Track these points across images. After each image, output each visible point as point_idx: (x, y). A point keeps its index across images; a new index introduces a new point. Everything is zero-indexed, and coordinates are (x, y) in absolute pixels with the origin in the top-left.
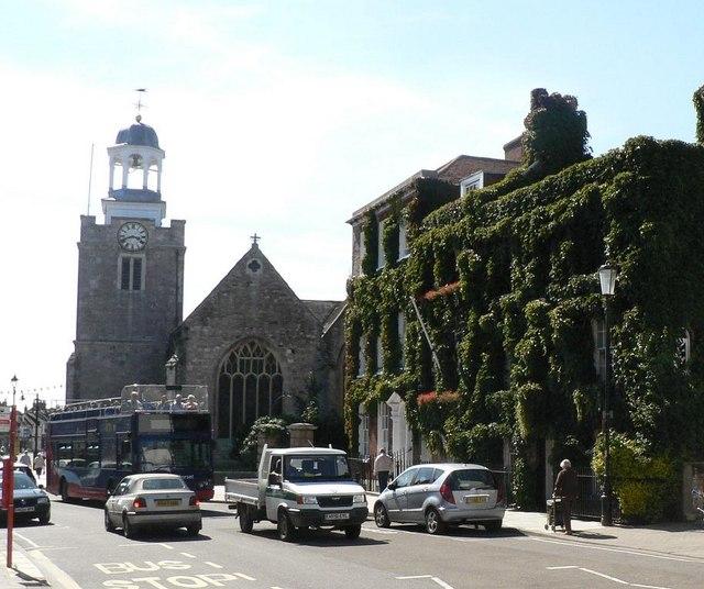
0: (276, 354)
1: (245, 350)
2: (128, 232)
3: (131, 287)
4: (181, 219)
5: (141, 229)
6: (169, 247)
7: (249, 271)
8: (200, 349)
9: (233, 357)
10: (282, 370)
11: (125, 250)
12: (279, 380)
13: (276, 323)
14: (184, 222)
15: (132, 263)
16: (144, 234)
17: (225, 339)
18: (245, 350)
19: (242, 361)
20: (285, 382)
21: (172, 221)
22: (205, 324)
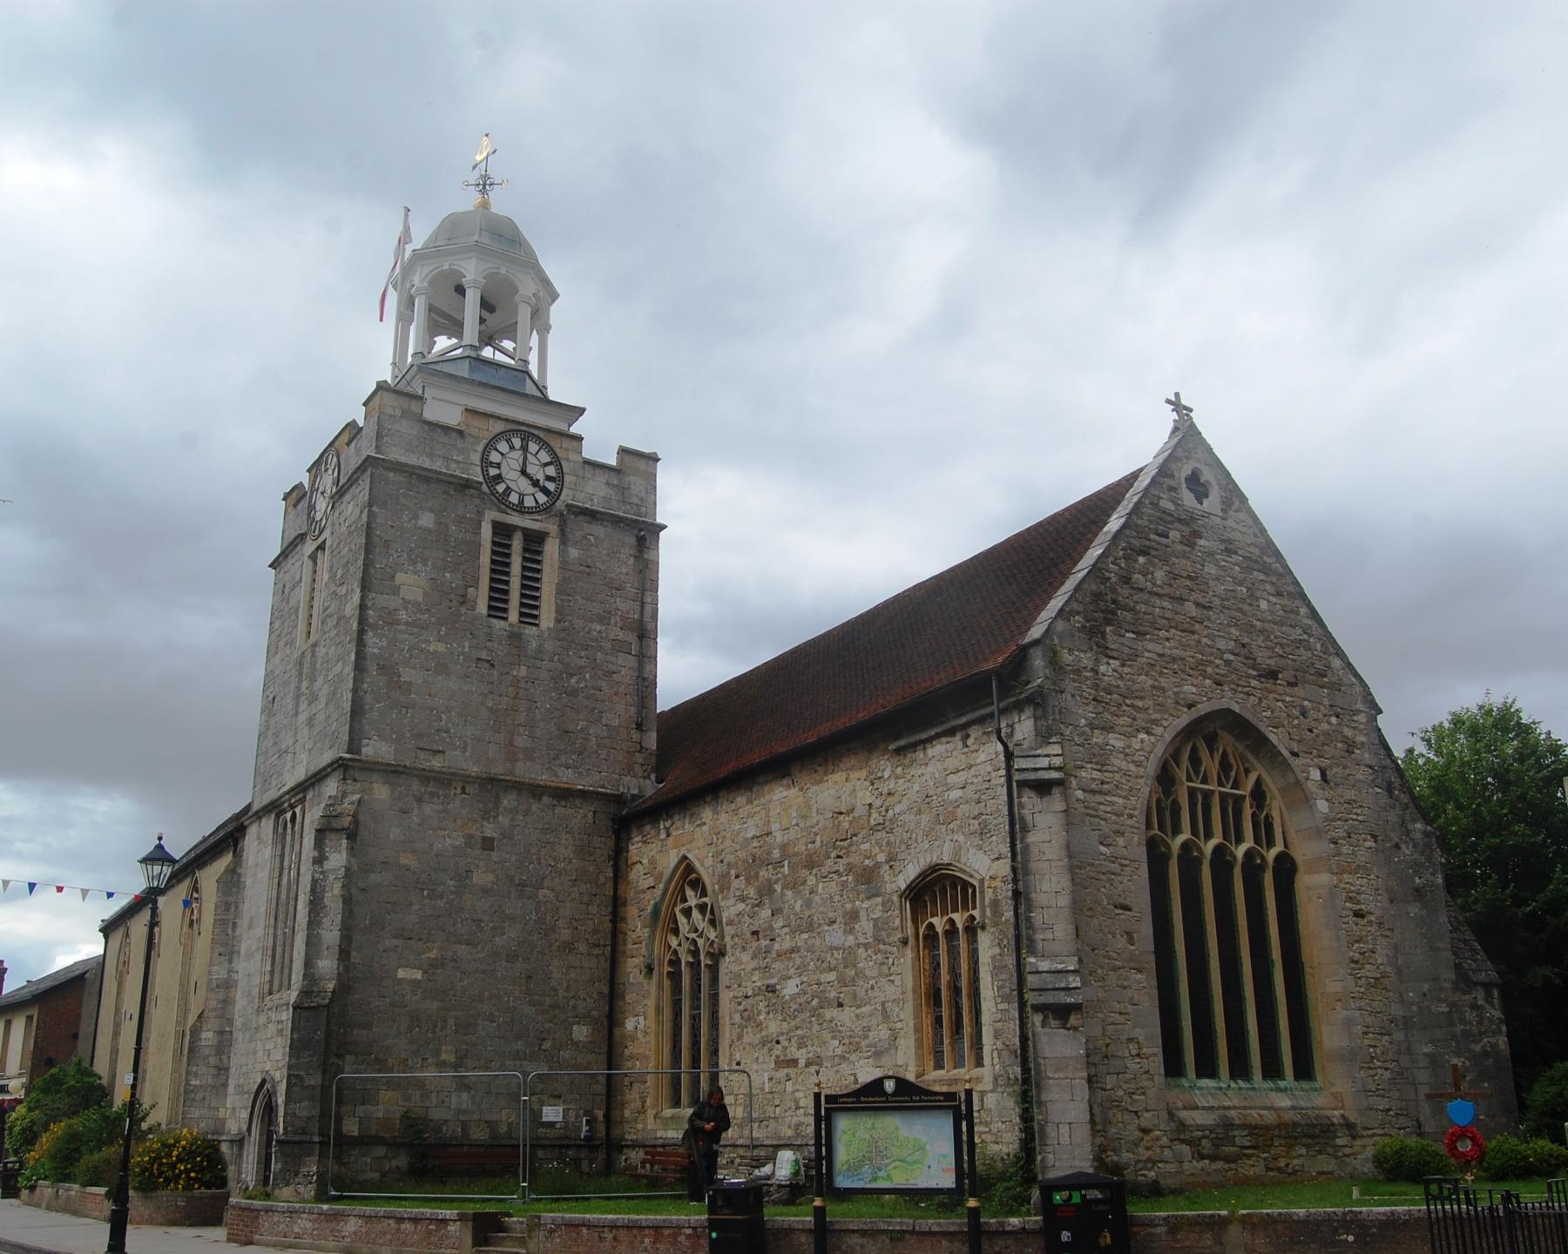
0: (1272, 785)
1: (1195, 761)
2: (509, 462)
3: (513, 616)
4: (646, 450)
5: (544, 457)
7: (1188, 498)
8: (1097, 738)
9: (1165, 778)
10: (1292, 835)
11: (502, 501)
12: (1286, 868)
13: (1272, 675)
14: (654, 459)
15: (517, 544)
16: (551, 471)
17: (1160, 706)
18: (1195, 761)
19: (1192, 792)
21: (624, 452)
22: (1105, 652)
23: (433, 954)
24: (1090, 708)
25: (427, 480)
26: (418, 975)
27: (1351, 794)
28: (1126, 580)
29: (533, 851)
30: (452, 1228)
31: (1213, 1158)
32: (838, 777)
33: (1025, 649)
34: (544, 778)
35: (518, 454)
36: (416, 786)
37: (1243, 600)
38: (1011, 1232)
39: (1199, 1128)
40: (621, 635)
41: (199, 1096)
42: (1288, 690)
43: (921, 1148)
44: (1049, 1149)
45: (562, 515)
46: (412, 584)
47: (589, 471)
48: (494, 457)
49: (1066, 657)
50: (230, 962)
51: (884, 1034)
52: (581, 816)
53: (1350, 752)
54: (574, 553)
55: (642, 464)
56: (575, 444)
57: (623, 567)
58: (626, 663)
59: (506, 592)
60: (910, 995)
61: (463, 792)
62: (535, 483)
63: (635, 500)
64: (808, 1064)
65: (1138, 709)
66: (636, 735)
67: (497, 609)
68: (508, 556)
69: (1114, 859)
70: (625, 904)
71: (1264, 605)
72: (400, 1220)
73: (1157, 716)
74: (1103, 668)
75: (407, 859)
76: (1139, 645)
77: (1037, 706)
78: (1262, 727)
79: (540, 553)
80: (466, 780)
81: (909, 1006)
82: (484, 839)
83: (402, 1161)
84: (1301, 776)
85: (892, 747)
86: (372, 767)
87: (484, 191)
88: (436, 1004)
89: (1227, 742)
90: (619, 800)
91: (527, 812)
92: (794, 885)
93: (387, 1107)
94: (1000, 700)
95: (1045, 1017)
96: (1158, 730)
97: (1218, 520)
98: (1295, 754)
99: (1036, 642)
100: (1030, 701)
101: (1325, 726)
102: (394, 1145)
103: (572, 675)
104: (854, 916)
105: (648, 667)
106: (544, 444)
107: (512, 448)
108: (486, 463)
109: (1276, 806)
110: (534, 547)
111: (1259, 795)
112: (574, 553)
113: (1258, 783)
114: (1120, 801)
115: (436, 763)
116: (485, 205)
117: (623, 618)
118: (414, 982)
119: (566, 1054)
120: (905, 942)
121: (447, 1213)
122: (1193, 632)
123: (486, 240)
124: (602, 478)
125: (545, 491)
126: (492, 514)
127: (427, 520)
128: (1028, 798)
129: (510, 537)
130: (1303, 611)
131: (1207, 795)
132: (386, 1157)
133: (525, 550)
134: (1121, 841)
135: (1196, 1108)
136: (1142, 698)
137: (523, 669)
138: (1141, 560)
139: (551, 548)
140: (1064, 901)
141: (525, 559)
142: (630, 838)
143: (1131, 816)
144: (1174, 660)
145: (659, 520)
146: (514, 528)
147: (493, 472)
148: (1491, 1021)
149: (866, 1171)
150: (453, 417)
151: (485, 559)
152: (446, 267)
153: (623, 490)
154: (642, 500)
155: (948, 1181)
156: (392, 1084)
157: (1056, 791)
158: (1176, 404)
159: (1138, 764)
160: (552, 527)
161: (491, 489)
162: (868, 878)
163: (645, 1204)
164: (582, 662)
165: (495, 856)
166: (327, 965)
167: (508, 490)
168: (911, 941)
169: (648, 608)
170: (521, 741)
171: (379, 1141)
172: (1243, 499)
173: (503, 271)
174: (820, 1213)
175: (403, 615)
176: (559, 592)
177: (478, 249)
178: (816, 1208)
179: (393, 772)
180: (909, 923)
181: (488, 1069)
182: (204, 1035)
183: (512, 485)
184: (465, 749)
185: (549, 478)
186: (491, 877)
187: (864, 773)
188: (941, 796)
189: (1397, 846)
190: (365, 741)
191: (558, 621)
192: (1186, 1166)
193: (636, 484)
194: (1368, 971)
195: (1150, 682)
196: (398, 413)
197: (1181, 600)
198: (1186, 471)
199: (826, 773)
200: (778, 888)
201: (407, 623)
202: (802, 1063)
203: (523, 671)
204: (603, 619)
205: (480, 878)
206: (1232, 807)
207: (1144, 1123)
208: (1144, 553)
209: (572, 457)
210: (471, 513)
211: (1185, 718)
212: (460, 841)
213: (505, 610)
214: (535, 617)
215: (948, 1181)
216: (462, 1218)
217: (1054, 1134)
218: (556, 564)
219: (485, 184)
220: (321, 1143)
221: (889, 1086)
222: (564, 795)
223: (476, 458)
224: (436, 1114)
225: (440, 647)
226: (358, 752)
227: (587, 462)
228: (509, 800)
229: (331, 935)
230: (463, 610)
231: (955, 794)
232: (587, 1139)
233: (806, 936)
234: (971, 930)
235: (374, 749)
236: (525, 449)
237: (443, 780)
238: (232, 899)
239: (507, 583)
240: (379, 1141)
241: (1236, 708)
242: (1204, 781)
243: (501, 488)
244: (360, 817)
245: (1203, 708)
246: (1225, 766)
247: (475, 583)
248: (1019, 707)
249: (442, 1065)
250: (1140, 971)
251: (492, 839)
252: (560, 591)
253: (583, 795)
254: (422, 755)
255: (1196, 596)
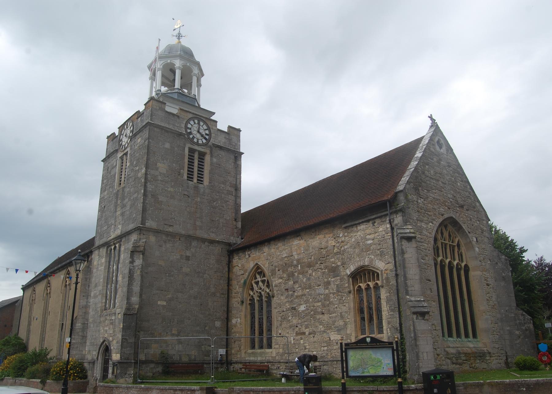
0: (462, 243)
1: (442, 234)
2: (194, 127)
3: (195, 180)
5: (205, 127)
6: (227, 149)
7: (437, 148)
9: (436, 240)
13: (462, 207)
14: (239, 130)
15: (196, 156)
16: (207, 132)
18: (442, 234)
20: (472, 274)
21: (230, 127)
23: (169, 296)
24: (417, 214)
25: (167, 132)
26: (165, 303)
27: (484, 246)
28: (423, 173)
29: (202, 261)
30: (197, 393)
31: (456, 364)
32: (321, 236)
33: (397, 193)
34: (206, 236)
35: (196, 125)
36: (164, 237)
37: (453, 182)
38: (412, 390)
39: (452, 354)
40: (230, 189)
41: (76, 346)
42: (467, 212)
43: (380, 361)
44: (420, 361)
45: (211, 147)
46: (162, 167)
47: (219, 133)
48: (189, 126)
49: (410, 197)
50: (87, 299)
51: (341, 323)
52: (217, 249)
53: (482, 233)
54: (215, 160)
55: (236, 132)
56: (215, 123)
57: (230, 166)
58: (231, 198)
59: (193, 172)
60: (352, 310)
61: (180, 239)
62: (202, 136)
63: (234, 144)
64: (310, 334)
65: (429, 215)
66: (234, 223)
67: (190, 178)
68: (193, 159)
69: (425, 264)
70: (231, 280)
71: (459, 184)
72: (176, 390)
73: (434, 218)
74: (419, 201)
75: (161, 263)
76: (428, 194)
77: (403, 212)
78: (461, 223)
79: (203, 159)
80: (180, 236)
81: (352, 314)
82: (186, 256)
83: (160, 369)
84: (471, 240)
85: (343, 226)
86: (150, 230)
87: (179, 39)
88: (171, 313)
89: (450, 227)
90: (229, 244)
91: (201, 247)
92: (302, 273)
93: (154, 350)
94: (390, 209)
95: (417, 316)
96: (435, 222)
97: (445, 156)
98: (469, 233)
99: (401, 191)
100: (401, 210)
101: (476, 224)
102: (157, 363)
103: (214, 202)
104: (328, 283)
105: (238, 200)
106: (205, 123)
107: (195, 123)
108: (186, 128)
109: (463, 249)
110: (201, 157)
111: (458, 245)
112: (215, 160)
113: (458, 242)
114: (426, 245)
115: (171, 229)
116: (180, 42)
117: (230, 183)
118: (163, 306)
119: (213, 331)
120: (350, 292)
121: (195, 387)
122: (442, 191)
123: (182, 53)
124: (223, 135)
125: (205, 139)
126: (188, 146)
127: (167, 145)
128: (404, 243)
129: (194, 153)
130: (468, 187)
131: (446, 244)
132: (154, 368)
133: (199, 158)
134: (427, 258)
135: (450, 347)
136: (430, 212)
137: (199, 198)
138: (427, 167)
139: (207, 158)
140: (417, 277)
141: (199, 161)
142: (233, 258)
143: (429, 250)
144: (437, 200)
145: (242, 150)
146: (196, 150)
147: (189, 131)
148: (528, 319)
149: (360, 370)
150: (175, 111)
151: (186, 160)
152: (169, 61)
153: (230, 140)
154: (236, 144)
155: (390, 373)
156: (156, 342)
157: (413, 240)
158: (431, 117)
159: (430, 233)
160: (208, 151)
161: (187, 136)
162: (334, 271)
163: (243, 383)
164: (218, 197)
165: (190, 262)
166: (135, 299)
167: (194, 137)
168: (352, 292)
169: (238, 180)
170: (198, 223)
171: (152, 362)
172: (452, 150)
173: (188, 64)
174: (344, 385)
175: (160, 178)
176: (210, 173)
177: (181, 57)
178: (342, 383)
179: (156, 232)
180: (351, 286)
181: (188, 336)
182: (77, 325)
183: (195, 136)
184: (180, 225)
185: (206, 134)
186: (189, 270)
187: (331, 235)
188: (367, 242)
189: (497, 263)
190: (147, 221)
191: (210, 183)
192: (449, 366)
193: (234, 138)
194: (491, 303)
195: (432, 207)
196: (158, 108)
197: (438, 180)
198: (436, 140)
199: (315, 235)
200: (296, 274)
201: (161, 181)
202: (307, 333)
203: (199, 199)
204: (224, 183)
205: (186, 270)
206: (452, 248)
207: (438, 353)
208: (428, 165)
209: (214, 128)
210: (176, 145)
211: (441, 220)
212: (179, 257)
213: (192, 178)
214: (202, 181)
215: (390, 373)
216: (201, 389)
217: (422, 356)
218: (209, 163)
219: (179, 36)
220: (135, 363)
221: (368, 340)
222: (212, 242)
223: (183, 126)
224: (171, 352)
225: (172, 190)
226: (145, 224)
227: (219, 130)
228: (194, 243)
229: (136, 288)
230: (179, 177)
231: (369, 242)
232: (220, 361)
233: (308, 290)
234: (377, 287)
235: (150, 224)
236: (199, 124)
237: (172, 236)
238: (88, 277)
239: (193, 169)
240: (152, 362)
241: (454, 217)
242: (444, 240)
243: (191, 136)
244: (146, 247)
245: (446, 216)
246: (450, 236)
247: (183, 168)
248: (396, 212)
249: (173, 335)
250: (434, 302)
251: (189, 257)
252: (211, 172)
253: (218, 242)
254: (166, 226)
255: (442, 180)
